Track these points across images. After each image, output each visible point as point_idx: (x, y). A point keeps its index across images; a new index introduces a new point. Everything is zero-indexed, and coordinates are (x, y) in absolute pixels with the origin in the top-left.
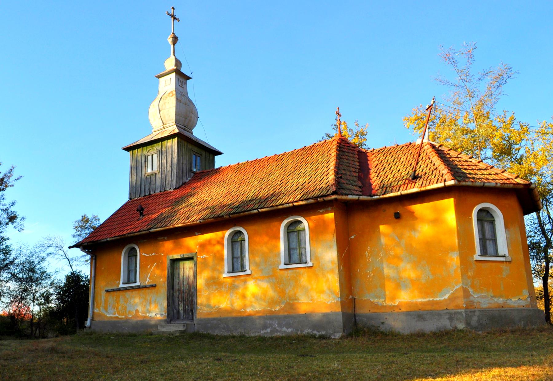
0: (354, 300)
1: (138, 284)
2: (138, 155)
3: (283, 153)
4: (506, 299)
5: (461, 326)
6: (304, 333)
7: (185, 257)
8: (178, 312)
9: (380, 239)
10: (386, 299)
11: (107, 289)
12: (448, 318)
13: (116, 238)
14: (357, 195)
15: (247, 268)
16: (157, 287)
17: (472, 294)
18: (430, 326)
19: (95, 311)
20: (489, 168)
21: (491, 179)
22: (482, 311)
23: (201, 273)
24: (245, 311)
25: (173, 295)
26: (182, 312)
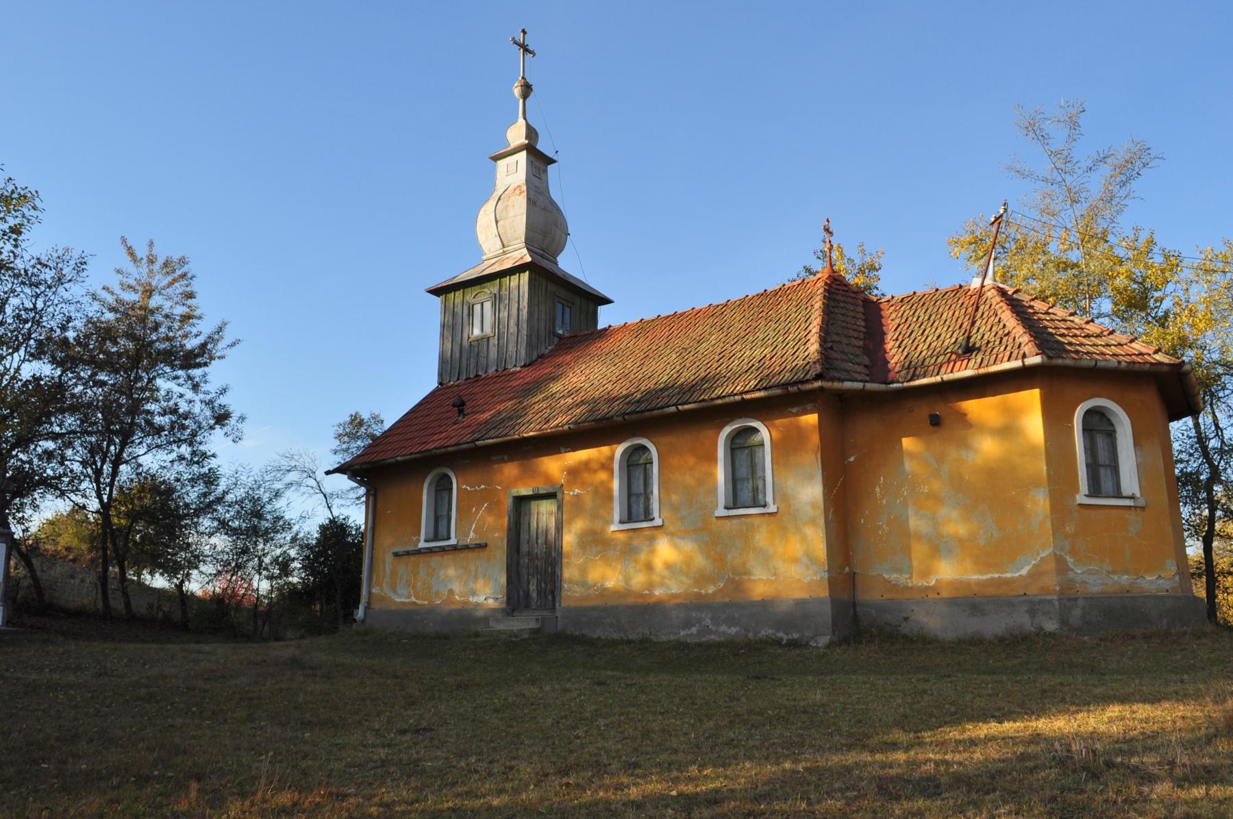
0: (853, 576)
1: (453, 541)
2: (456, 303)
3: (723, 301)
4: (1135, 577)
5: (1051, 626)
6: (760, 635)
7: (541, 492)
8: (527, 594)
9: (903, 464)
10: (912, 574)
11: (396, 550)
12: (1027, 611)
13: (413, 456)
14: (861, 381)
15: (656, 514)
16: (487, 549)
17: (1072, 567)
18: (993, 625)
19: (374, 591)
20: (1105, 333)
21: (1109, 354)
22: (1091, 599)
23: (571, 521)
24: (651, 595)
25: (518, 563)
26: (534, 595)
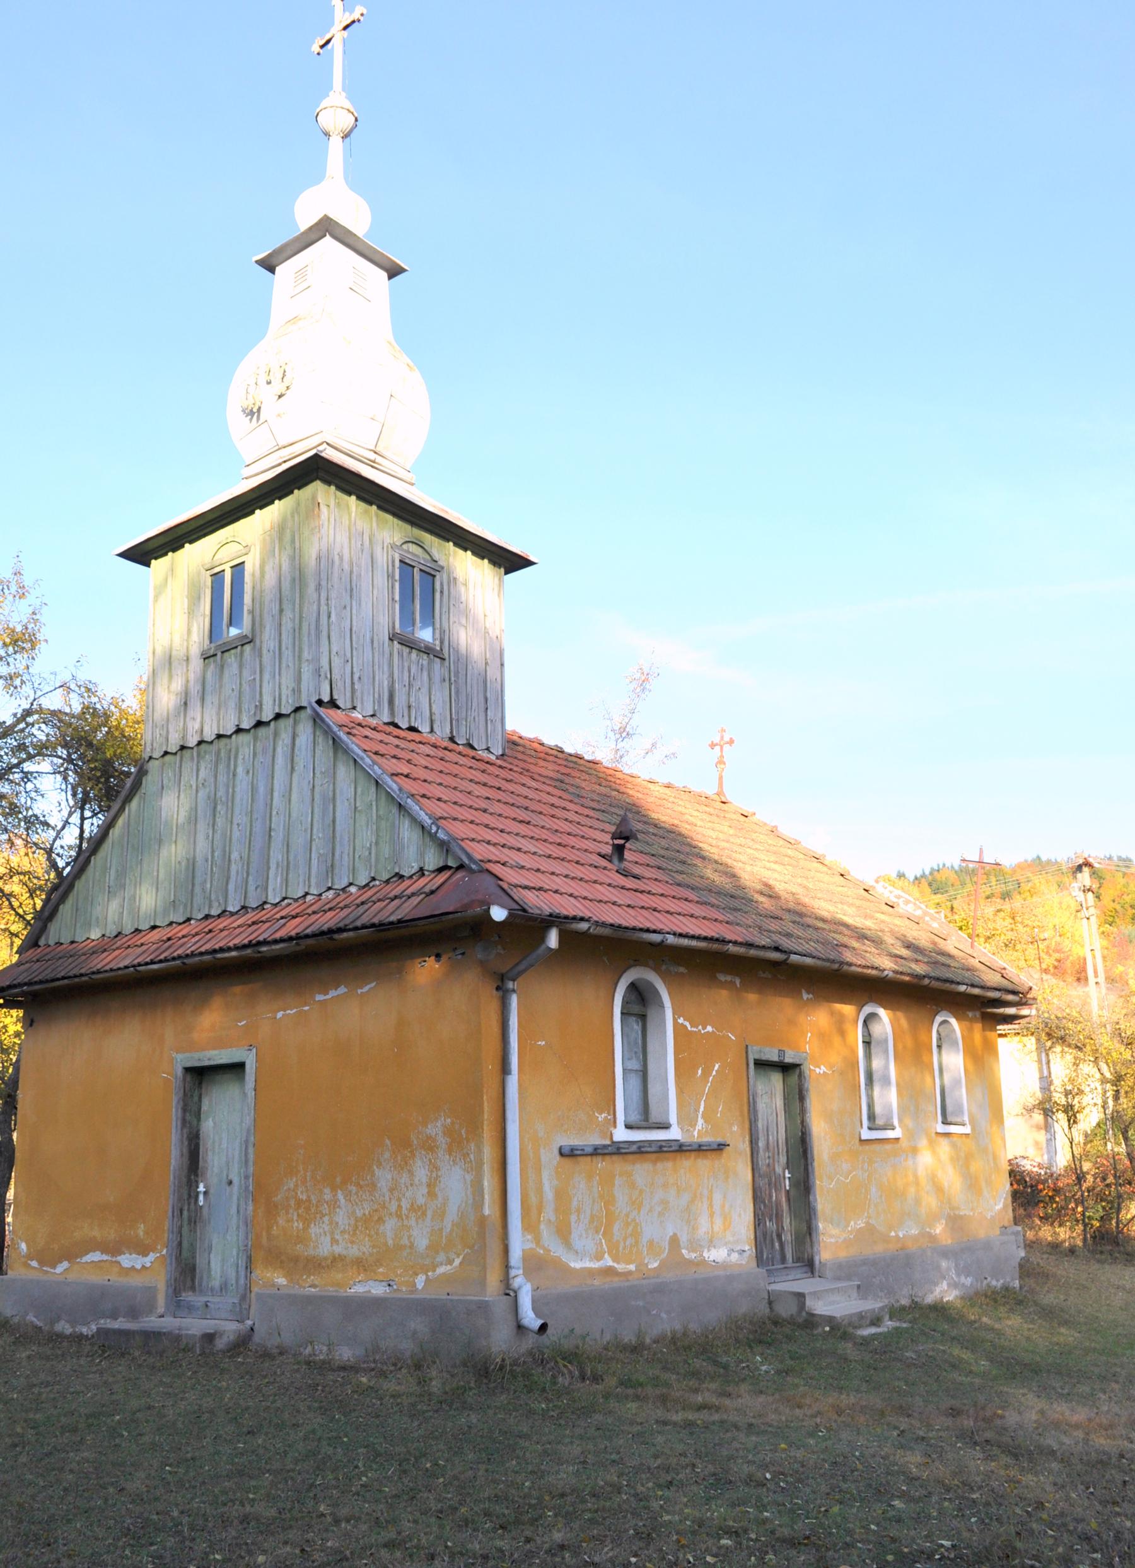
1: (674, 1133)
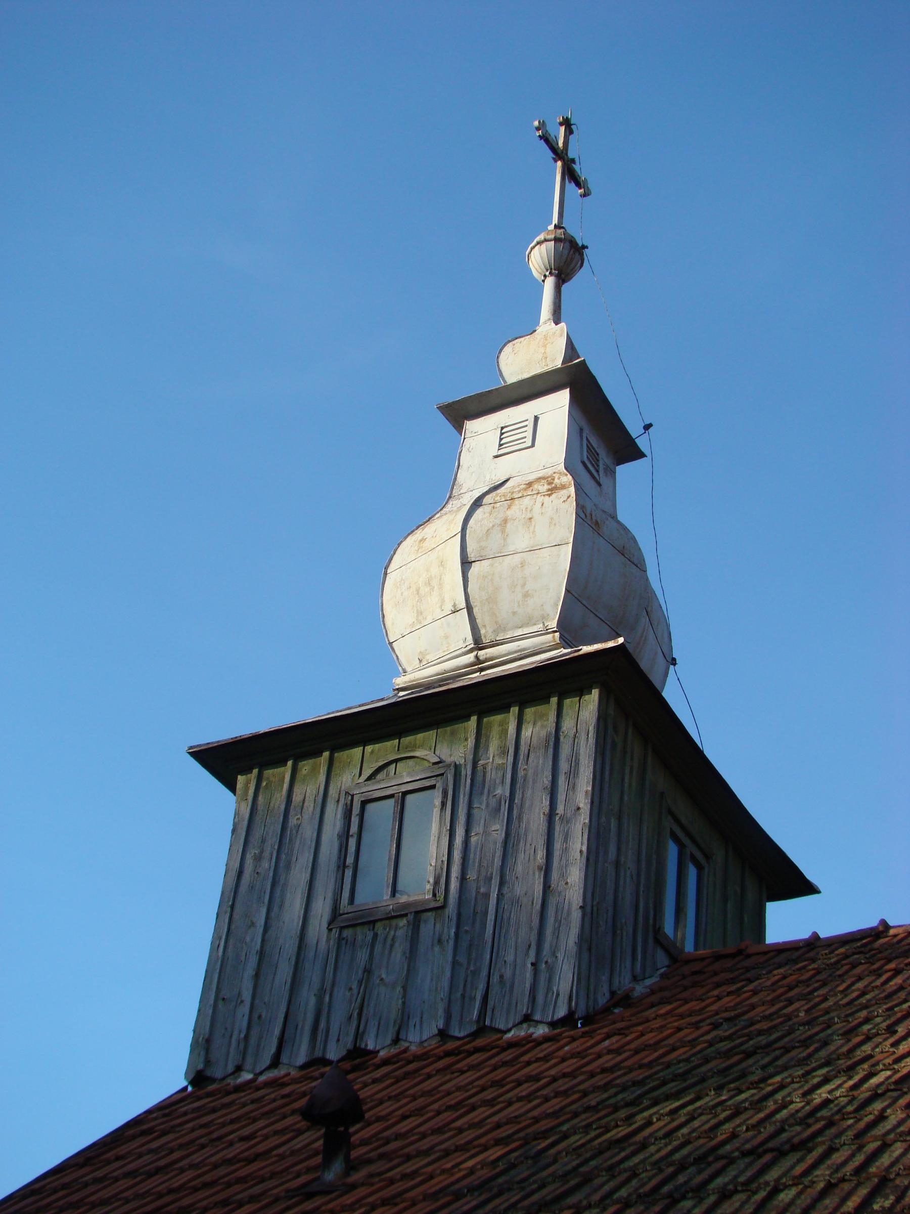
2: (297, 798)
